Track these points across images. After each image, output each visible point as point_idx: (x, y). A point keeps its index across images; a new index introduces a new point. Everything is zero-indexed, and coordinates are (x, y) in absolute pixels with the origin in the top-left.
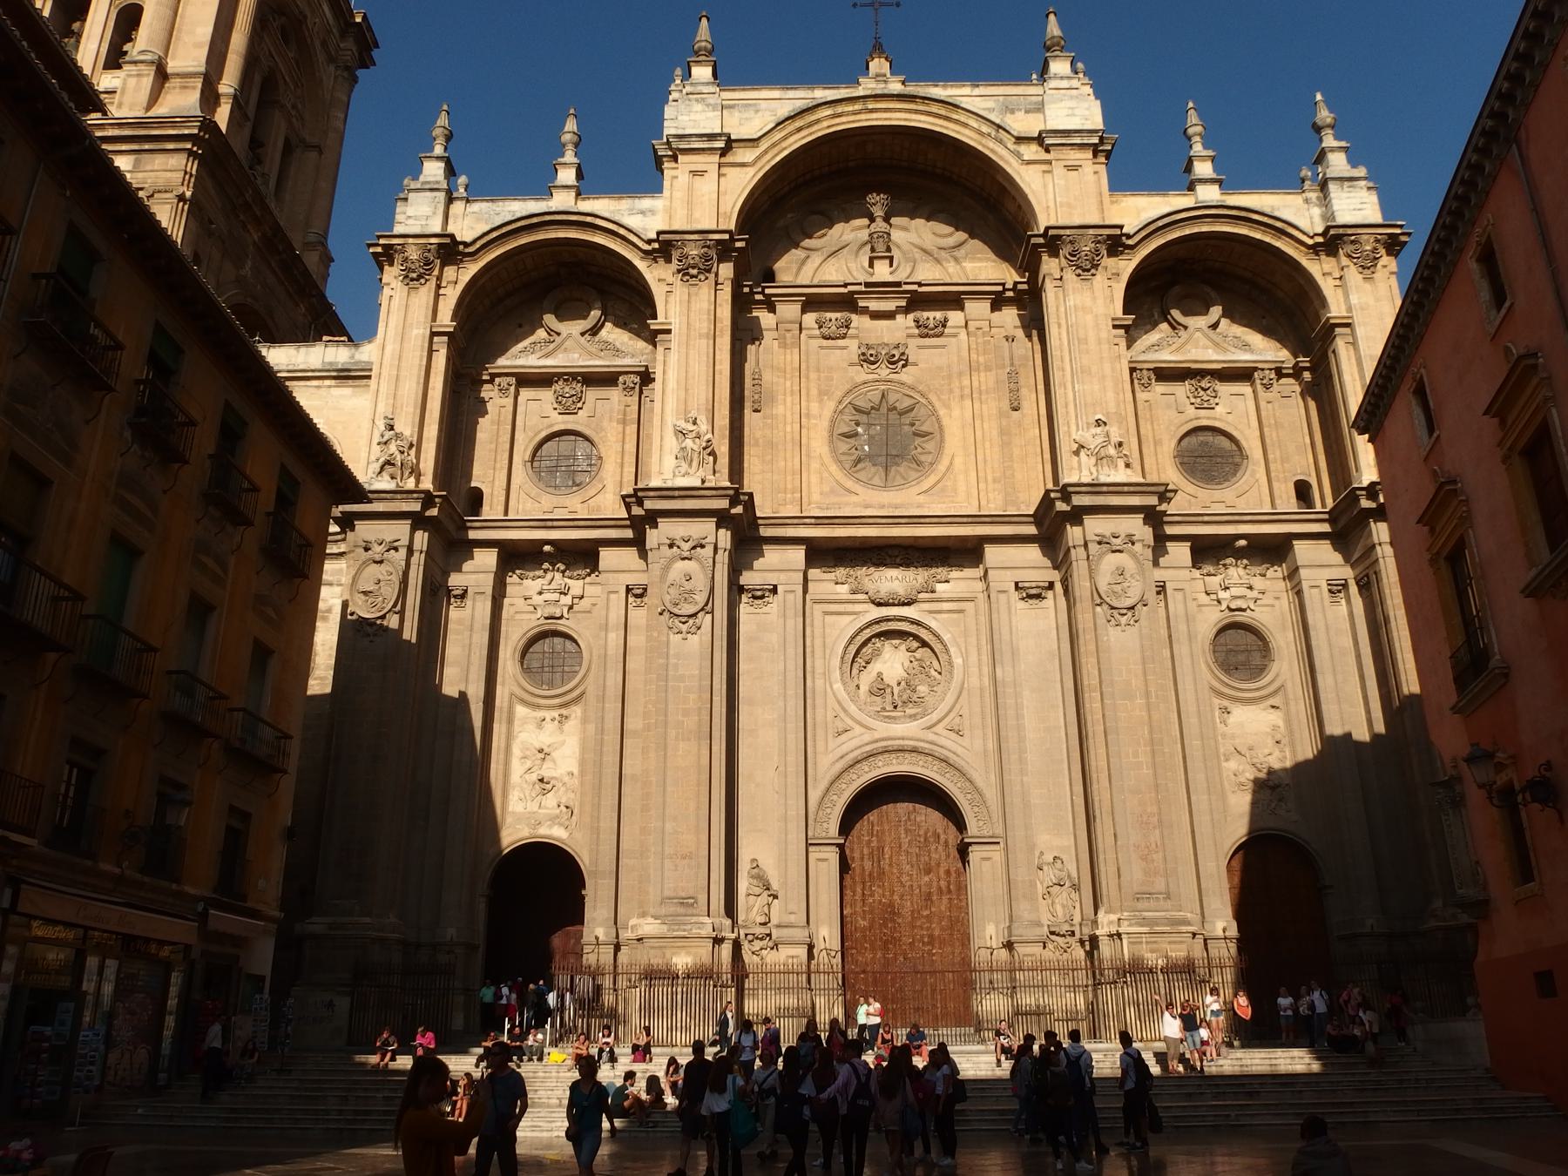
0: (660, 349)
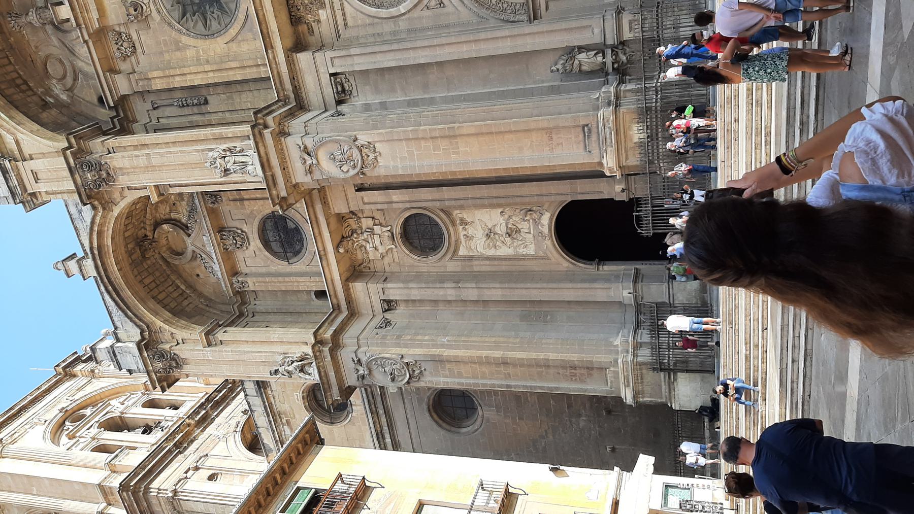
0: (172, 190)
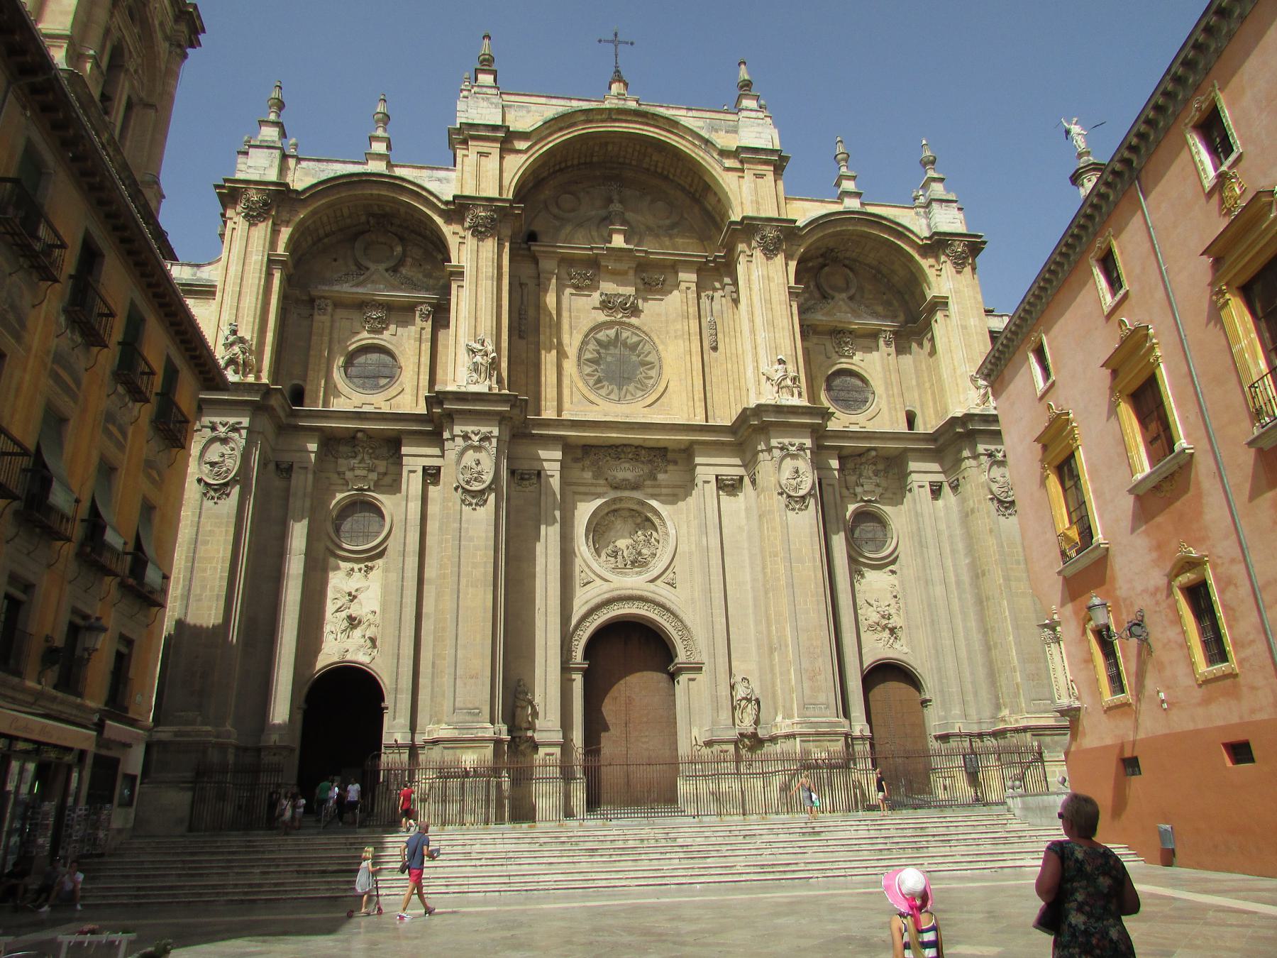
0: (454, 286)
